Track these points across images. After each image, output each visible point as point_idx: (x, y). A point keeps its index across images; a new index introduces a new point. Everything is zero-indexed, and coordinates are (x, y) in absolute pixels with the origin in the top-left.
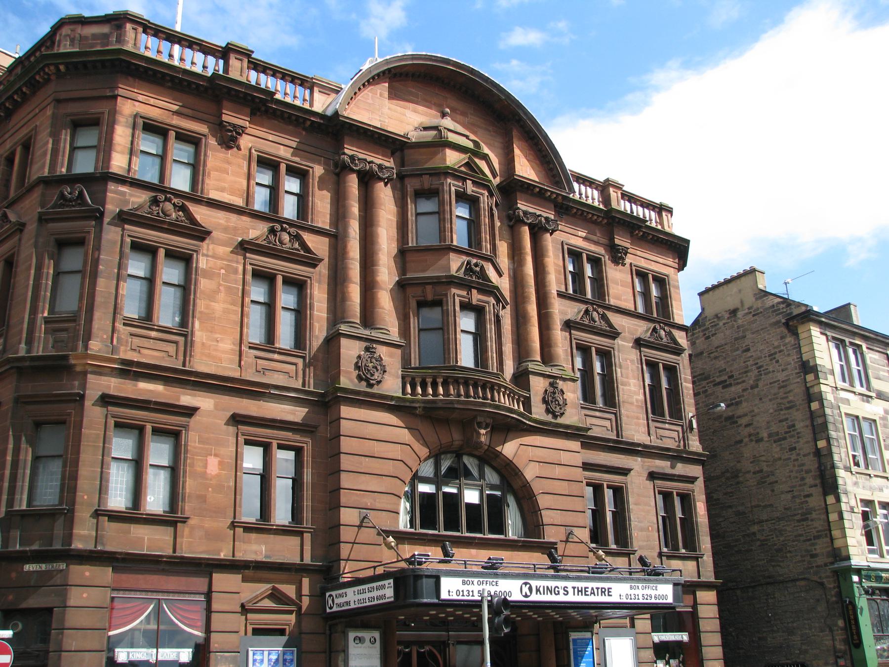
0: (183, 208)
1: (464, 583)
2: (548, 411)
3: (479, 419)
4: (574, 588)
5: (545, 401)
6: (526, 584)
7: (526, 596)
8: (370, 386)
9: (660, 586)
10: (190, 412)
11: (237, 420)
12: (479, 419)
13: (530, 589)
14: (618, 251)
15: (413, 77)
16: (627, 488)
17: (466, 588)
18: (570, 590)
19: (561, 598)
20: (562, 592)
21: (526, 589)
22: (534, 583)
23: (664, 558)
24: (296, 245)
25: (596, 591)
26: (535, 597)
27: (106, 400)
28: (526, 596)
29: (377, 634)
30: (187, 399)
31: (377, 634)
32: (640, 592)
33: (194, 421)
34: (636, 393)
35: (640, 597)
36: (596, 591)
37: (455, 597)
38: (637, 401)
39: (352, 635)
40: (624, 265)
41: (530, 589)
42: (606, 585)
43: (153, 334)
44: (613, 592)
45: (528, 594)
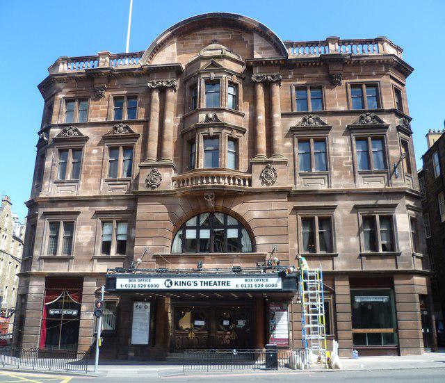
0: (76, 130)
1: (130, 281)
2: (263, 183)
3: (205, 194)
4: (201, 282)
5: (261, 177)
6: (168, 280)
7: (168, 287)
8: (154, 188)
9: (269, 279)
10: (78, 213)
11: (98, 213)
12: (205, 194)
13: (171, 283)
14: (333, 78)
15: (187, 30)
16: (333, 216)
17: (131, 283)
18: (199, 283)
19: (192, 287)
20: (193, 284)
21: (168, 283)
22: (173, 280)
23: (364, 258)
24: (127, 131)
25: (218, 283)
26: (174, 287)
27: (45, 214)
28: (168, 287)
29: (148, 305)
30: (76, 209)
31: (148, 305)
32: (253, 283)
33: (79, 217)
34: (345, 159)
35: (253, 286)
36: (218, 283)
37: (124, 288)
38: (346, 164)
39: (135, 305)
40: (340, 84)
41: (171, 283)
42: (226, 280)
43: (66, 184)
44: (231, 283)
45: (170, 285)
